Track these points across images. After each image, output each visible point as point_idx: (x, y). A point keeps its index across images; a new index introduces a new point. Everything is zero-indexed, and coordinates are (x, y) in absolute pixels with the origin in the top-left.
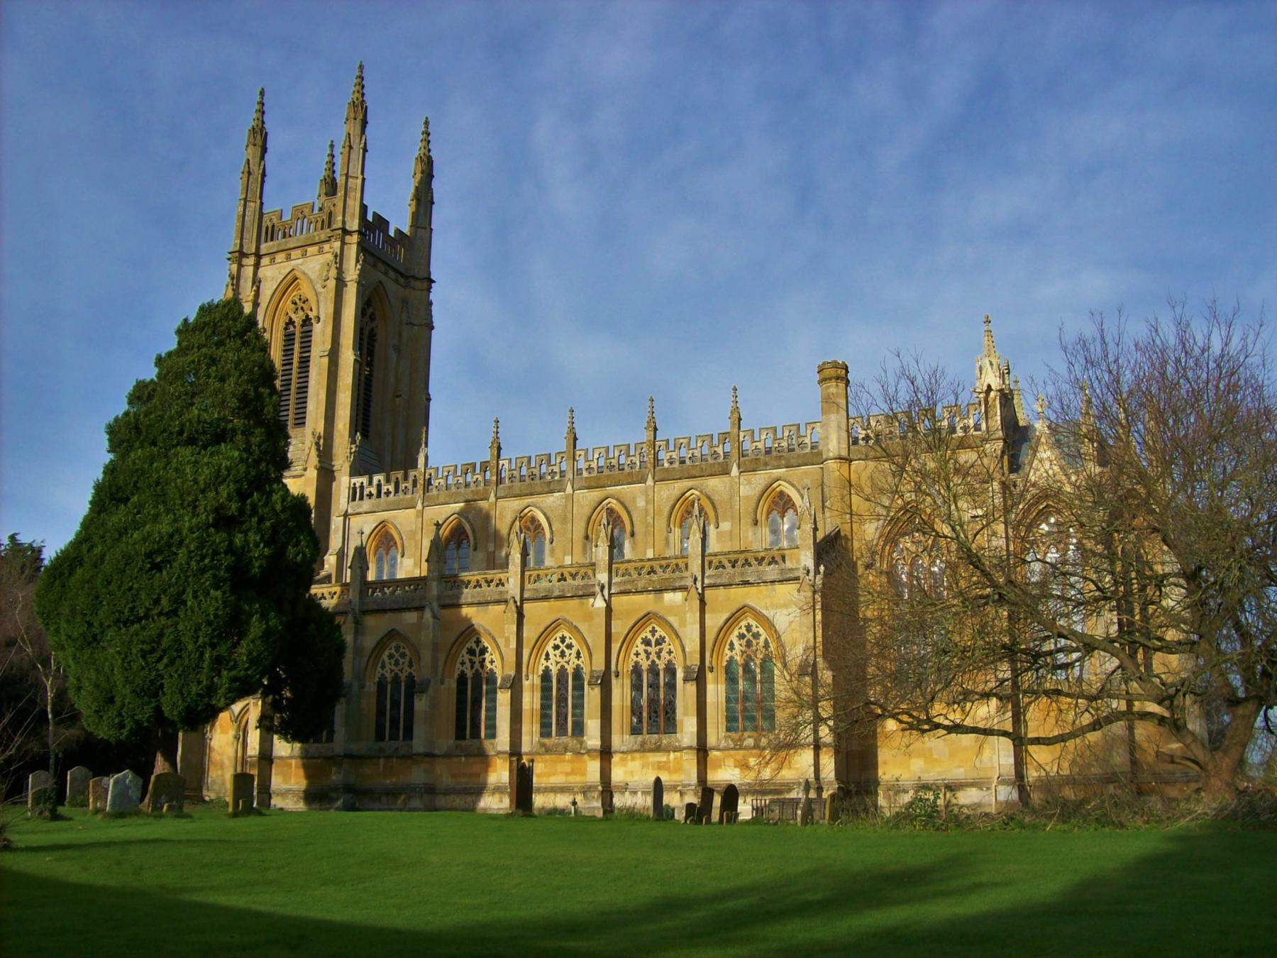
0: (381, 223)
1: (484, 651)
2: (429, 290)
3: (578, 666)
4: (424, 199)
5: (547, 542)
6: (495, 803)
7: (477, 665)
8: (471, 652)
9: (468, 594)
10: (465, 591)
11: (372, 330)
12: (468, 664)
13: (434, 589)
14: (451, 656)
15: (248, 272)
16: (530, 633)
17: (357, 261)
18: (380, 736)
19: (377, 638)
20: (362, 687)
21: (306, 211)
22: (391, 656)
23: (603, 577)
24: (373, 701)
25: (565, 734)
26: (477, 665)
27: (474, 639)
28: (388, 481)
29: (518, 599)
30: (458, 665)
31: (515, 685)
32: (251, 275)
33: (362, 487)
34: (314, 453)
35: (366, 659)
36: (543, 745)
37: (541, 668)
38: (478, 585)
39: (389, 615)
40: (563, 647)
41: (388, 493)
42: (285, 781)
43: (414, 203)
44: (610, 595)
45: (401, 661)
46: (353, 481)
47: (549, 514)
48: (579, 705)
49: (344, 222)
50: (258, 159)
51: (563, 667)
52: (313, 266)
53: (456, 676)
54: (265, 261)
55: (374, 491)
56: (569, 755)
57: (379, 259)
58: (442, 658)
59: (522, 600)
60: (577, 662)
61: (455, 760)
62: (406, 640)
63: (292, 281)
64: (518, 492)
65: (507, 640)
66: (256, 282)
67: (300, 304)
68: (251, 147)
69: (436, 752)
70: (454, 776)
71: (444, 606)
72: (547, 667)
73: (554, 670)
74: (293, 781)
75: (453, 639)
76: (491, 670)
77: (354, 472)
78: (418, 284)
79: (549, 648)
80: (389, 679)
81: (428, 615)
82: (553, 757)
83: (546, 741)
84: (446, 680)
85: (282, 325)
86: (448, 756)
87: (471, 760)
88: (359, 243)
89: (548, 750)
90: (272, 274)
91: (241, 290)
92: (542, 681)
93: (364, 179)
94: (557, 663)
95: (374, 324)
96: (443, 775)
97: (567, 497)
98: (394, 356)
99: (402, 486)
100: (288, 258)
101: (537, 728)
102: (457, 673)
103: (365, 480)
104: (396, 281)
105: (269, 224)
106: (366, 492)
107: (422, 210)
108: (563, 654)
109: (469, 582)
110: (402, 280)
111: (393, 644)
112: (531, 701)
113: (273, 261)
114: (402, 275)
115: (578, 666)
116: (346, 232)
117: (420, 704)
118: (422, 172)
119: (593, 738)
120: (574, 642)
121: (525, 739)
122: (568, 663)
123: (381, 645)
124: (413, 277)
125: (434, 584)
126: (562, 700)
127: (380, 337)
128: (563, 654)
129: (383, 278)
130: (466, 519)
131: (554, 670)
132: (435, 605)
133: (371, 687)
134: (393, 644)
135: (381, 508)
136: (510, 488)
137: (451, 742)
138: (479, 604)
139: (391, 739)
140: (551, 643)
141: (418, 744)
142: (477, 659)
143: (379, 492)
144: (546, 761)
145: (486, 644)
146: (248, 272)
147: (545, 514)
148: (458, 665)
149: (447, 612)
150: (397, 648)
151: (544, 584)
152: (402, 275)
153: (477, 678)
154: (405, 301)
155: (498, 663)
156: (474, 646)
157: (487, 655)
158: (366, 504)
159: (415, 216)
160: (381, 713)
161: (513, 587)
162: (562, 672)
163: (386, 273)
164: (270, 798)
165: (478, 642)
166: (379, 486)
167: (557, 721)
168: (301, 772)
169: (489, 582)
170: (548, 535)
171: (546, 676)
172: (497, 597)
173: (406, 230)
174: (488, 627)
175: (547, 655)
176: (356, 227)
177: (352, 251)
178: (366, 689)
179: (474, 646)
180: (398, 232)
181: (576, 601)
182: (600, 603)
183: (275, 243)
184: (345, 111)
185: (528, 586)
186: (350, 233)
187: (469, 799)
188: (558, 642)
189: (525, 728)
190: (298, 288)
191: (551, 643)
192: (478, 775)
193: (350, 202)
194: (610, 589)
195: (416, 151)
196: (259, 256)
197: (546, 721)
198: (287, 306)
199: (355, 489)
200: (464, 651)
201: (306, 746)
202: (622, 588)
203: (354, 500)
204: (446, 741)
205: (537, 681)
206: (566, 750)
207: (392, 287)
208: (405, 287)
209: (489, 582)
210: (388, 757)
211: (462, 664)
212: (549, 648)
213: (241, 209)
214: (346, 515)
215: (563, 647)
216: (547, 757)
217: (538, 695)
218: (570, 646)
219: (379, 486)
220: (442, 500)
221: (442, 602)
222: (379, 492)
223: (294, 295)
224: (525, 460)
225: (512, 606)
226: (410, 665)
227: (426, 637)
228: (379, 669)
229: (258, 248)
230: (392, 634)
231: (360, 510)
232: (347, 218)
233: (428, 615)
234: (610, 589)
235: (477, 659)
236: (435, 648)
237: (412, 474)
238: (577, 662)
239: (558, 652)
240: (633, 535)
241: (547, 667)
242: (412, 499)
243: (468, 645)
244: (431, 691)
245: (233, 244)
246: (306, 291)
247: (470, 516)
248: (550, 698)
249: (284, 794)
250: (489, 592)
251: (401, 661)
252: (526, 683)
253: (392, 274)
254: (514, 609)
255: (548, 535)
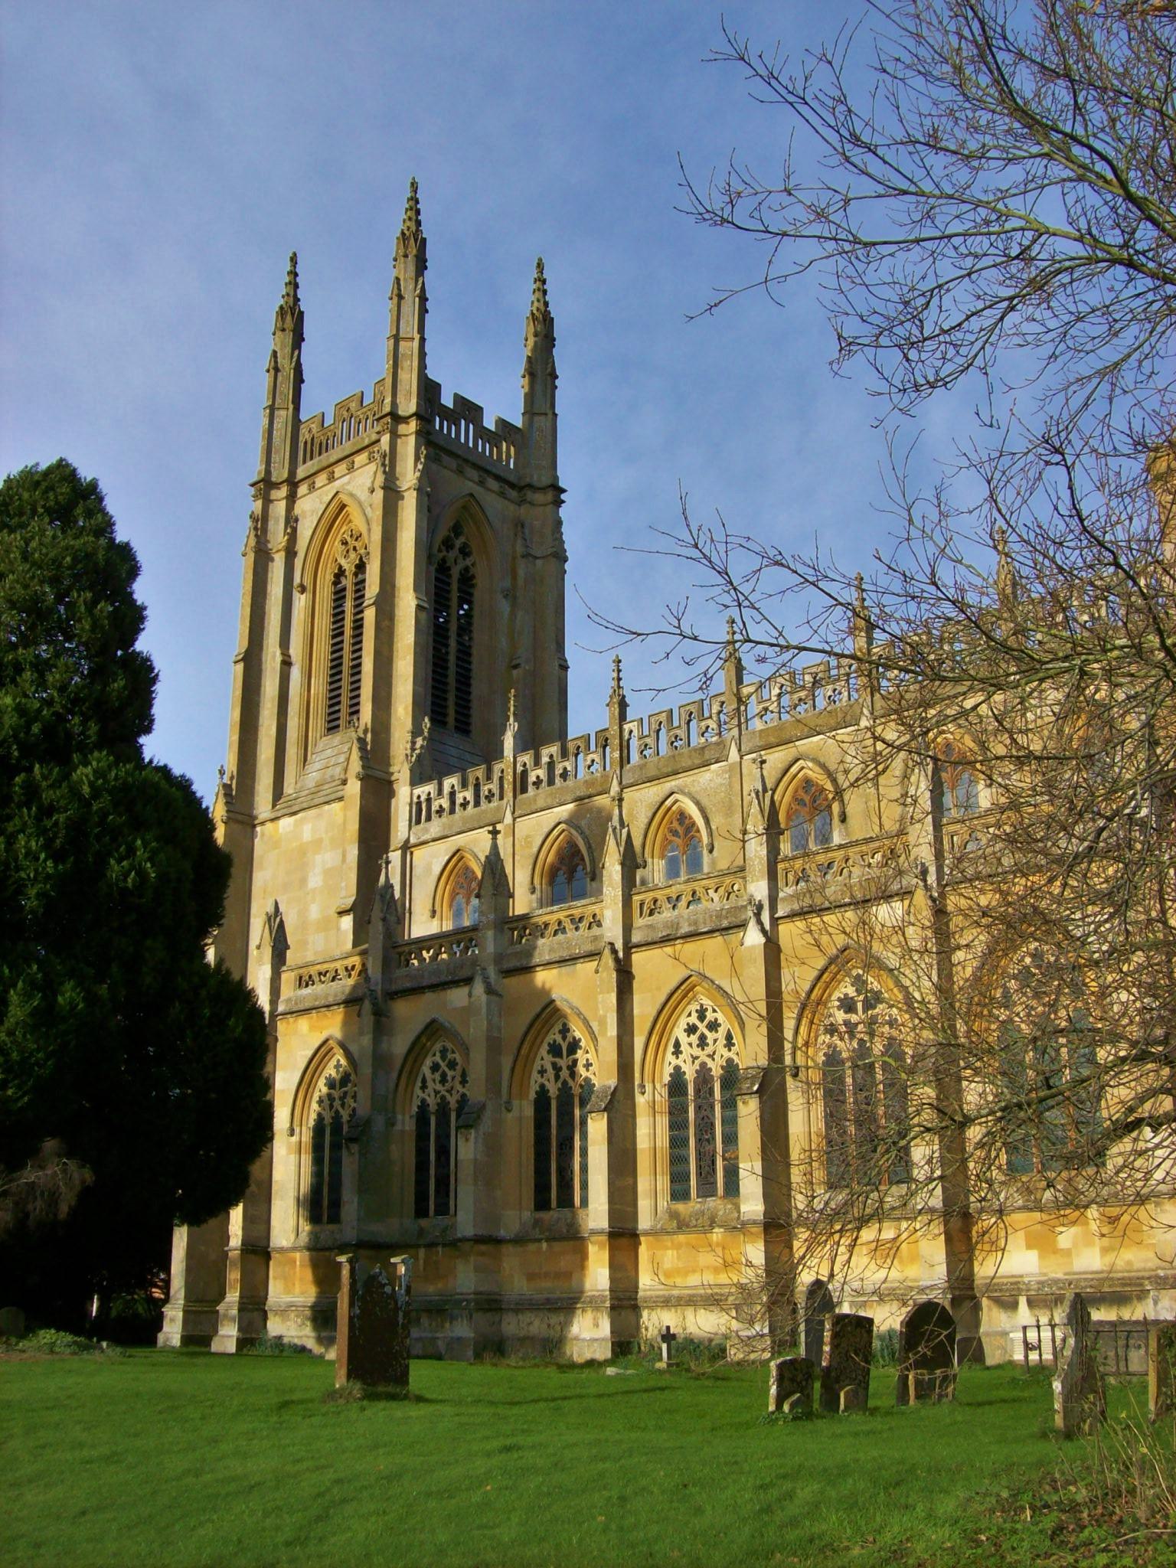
0: (468, 410)
1: (574, 1046)
2: (559, 503)
3: (730, 1061)
4: (541, 373)
5: (705, 852)
6: (589, 1333)
7: (565, 1074)
8: (555, 1050)
9: (545, 947)
10: (541, 942)
11: (467, 569)
12: (551, 1073)
13: (490, 942)
14: (522, 1060)
15: (279, 508)
16: (644, 1007)
17: (417, 459)
18: (421, 1211)
19: (411, 1037)
20: (391, 1123)
21: (353, 405)
22: (435, 1068)
23: (759, 889)
24: (411, 1146)
25: (713, 1193)
26: (565, 1074)
27: (559, 1027)
28: (464, 785)
29: (619, 946)
30: (535, 1075)
31: (620, 1108)
32: (283, 513)
33: (429, 800)
34: (355, 755)
35: (395, 1075)
36: (673, 1215)
37: (668, 1070)
38: (561, 929)
39: (429, 996)
40: (702, 1027)
41: (464, 805)
42: (288, 1291)
43: (526, 381)
44: (775, 921)
45: (450, 1073)
46: (416, 792)
47: (705, 802)
48: (731, 1139)
49: (394, 404)
50: (288, 349)
51: (703, 1065)
52: (360, 482)
53: (532, 1095)
54: (303, 489)
55: (445, 803)
56: (717, 1234)
57: (466, 461)
58: (506, 1062)
59: (629, 947)
60: (727, 1054)
61: (532, 1247)
62: (453, 1035)
63: (338, 510)
64: (652, 772)
65: (602, 1022)
66: (292, 521)
67: (352, 542)
68: (279, 333)
69: (502, 1233)
70: (531, 1277)
71: (509, 973)
72: (677, 1068)
73: (690, 1072)
74: (297, 1290)
75: (523, 1029)
76: (587, 1080)
77: (418, 778)
78: (539, 497)
79: (679, 1032)
80: (433, 1108)
81: (479, 988)
82: (692, 1238)
83: (680, 1207)
84: (516, 1103)
85: (330, 578)
86: (519, 1241)
87: (558, 1246)
88: (418, 433)
89: (682, 1225)
90: (310, 506)
91: (270, 536)
92: (670, 1095)
93: (423, 340)
94: (695, 1058)
95: (468, 562)
96: (515, 1276)
97: (731, 767)
98: (505, 607)
99: (485, 790)
100: (331, 478)
101: (664, 1183)
102: (534, 1088)
103: (430, 788)
104: (502, 494)
105: (308, 437)
106: (435, 807)
107: (538, 388)
108: (703, 1042)
109: (546, 925)
110: (513, 494)
111: (438, 1046)
112: (650, 1132)
113: (312, 488)
114: (512, 486)
115: (730, 1061)
116: (396, 418)
117: (466, 1149)
118: (536, 335)
119: (752, 1203)
120: (720, 1017)
121: (644, 1205)
122: (712, 1056)
123: (417, 1050)
124: (530, 486)
125: (490, 934)
126: (705, 1127)
127: (481, 582)
128: (703, 1042)
129: (478, 490)
130: (578, 828)
131: (690, 1072)
132: (492, 972)
133: (406, 1123)
134: (438, 1046)
135: (456, 829)
136: (642, 767)
137: (527, 1215)
138: (562, 962)
139: (438, 1213)
140: (682, 1024)
141: (465, 1221)
142: (563, 1063)
143: (453, 802)
144: (678, 1247)
145: (578, 1034)
146: (279, 508)
147: (698, 803)
148: (535, 1075)
149: (513, 982)
150: (444, 1052)
151: (667, 914)
152: (512, 486)
153: (565, 1093)
154: (520, 525)
155: (597, 1066)
156: (559, 1038)
157: (580, 1052)
158: (435, 827)
159: (530, 399)
160: (422, 1167)
161: (612, 929)
162: (704, 1073)
163: (481, 483)
164: (265, 1318)
165: (565, 1030)
166: (452, 794)
167: (699, 1167)
168: (308, 1274)
169: (577, 921)
170: (705, 840)
171: (677, 1085)
172: (588, 947)
173: (518, 421)
174: (576, 1002)
175: (677, 1045)
176: (412, 407)
177: (408, 447)
178: (398, 1127)
179: (559, 1038)
180: (502, 423)
181: (718, 940)
182: (753, 938)
183: (315, 460)
184: (392, 247)
185: (639, 922)
186: (405, 420)
187: (555, 1319)
188: (694, 1019)
189: (643, 1184)
190: (348, 520)
191: (682, 1024)
192: (568, 1275)
193: (403, 376)
194: (773, 908)
195: (525, 302)
196: (293, 484)
197: (679, 1168)
198: (334, 548)
199: (419, 804)
200: (544, 1050)
201: (318, 1228)
202: (796, 907)
203: (418, 822)
204: (516, 1216)
205: (662, 1095)
206: (713, 1223)
207: (494, 504)
208: (521, 502)
209: (577, 921)
210: (431, 1245)
211: (541, 1076)
212: (679, 1032)
213: (266, 421)
214: (406, 847)
215: (702, 1027)
216: (681, 1238)
217: (663, 1122)
218: (713, 1026)
219: (452, 794)
220: (541, 803)
221: (506, 966)
222: (453, 802)
223: (341, 531)
224: (663, 717)
225: (608, 959)
226: (464, 1082)
227: (476, 1031)
228: (418, 1091)
229: (292, 472)
230: (432, 1029)
231: (424, 838)
232: (400, 399)
233: (479, 988)
234: (773, 908)
235: (563, 1063)
236: (494, 1046)
237: (497, 768)
238: (727, 1054)
239: (694, 1039)
240: (843, 819)
241: (677, 1068)
242: (498, 808)
243: (550, 1038)
244: (486, 1124)
245: (257, 470)
246: (358, 523)
247: (583, 823)
248: (684, 1125)
249: (284, 1312)
250: (577, 939)
251: (450, 1073)
252: (641, 1100)
253: (493, 484)
254: (611, 963)
255: (705, 840)
